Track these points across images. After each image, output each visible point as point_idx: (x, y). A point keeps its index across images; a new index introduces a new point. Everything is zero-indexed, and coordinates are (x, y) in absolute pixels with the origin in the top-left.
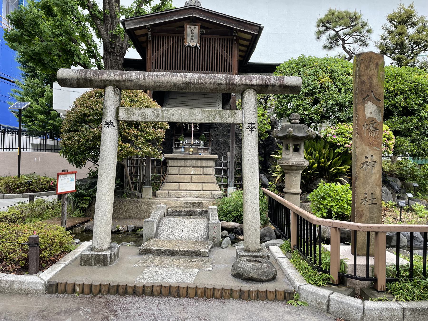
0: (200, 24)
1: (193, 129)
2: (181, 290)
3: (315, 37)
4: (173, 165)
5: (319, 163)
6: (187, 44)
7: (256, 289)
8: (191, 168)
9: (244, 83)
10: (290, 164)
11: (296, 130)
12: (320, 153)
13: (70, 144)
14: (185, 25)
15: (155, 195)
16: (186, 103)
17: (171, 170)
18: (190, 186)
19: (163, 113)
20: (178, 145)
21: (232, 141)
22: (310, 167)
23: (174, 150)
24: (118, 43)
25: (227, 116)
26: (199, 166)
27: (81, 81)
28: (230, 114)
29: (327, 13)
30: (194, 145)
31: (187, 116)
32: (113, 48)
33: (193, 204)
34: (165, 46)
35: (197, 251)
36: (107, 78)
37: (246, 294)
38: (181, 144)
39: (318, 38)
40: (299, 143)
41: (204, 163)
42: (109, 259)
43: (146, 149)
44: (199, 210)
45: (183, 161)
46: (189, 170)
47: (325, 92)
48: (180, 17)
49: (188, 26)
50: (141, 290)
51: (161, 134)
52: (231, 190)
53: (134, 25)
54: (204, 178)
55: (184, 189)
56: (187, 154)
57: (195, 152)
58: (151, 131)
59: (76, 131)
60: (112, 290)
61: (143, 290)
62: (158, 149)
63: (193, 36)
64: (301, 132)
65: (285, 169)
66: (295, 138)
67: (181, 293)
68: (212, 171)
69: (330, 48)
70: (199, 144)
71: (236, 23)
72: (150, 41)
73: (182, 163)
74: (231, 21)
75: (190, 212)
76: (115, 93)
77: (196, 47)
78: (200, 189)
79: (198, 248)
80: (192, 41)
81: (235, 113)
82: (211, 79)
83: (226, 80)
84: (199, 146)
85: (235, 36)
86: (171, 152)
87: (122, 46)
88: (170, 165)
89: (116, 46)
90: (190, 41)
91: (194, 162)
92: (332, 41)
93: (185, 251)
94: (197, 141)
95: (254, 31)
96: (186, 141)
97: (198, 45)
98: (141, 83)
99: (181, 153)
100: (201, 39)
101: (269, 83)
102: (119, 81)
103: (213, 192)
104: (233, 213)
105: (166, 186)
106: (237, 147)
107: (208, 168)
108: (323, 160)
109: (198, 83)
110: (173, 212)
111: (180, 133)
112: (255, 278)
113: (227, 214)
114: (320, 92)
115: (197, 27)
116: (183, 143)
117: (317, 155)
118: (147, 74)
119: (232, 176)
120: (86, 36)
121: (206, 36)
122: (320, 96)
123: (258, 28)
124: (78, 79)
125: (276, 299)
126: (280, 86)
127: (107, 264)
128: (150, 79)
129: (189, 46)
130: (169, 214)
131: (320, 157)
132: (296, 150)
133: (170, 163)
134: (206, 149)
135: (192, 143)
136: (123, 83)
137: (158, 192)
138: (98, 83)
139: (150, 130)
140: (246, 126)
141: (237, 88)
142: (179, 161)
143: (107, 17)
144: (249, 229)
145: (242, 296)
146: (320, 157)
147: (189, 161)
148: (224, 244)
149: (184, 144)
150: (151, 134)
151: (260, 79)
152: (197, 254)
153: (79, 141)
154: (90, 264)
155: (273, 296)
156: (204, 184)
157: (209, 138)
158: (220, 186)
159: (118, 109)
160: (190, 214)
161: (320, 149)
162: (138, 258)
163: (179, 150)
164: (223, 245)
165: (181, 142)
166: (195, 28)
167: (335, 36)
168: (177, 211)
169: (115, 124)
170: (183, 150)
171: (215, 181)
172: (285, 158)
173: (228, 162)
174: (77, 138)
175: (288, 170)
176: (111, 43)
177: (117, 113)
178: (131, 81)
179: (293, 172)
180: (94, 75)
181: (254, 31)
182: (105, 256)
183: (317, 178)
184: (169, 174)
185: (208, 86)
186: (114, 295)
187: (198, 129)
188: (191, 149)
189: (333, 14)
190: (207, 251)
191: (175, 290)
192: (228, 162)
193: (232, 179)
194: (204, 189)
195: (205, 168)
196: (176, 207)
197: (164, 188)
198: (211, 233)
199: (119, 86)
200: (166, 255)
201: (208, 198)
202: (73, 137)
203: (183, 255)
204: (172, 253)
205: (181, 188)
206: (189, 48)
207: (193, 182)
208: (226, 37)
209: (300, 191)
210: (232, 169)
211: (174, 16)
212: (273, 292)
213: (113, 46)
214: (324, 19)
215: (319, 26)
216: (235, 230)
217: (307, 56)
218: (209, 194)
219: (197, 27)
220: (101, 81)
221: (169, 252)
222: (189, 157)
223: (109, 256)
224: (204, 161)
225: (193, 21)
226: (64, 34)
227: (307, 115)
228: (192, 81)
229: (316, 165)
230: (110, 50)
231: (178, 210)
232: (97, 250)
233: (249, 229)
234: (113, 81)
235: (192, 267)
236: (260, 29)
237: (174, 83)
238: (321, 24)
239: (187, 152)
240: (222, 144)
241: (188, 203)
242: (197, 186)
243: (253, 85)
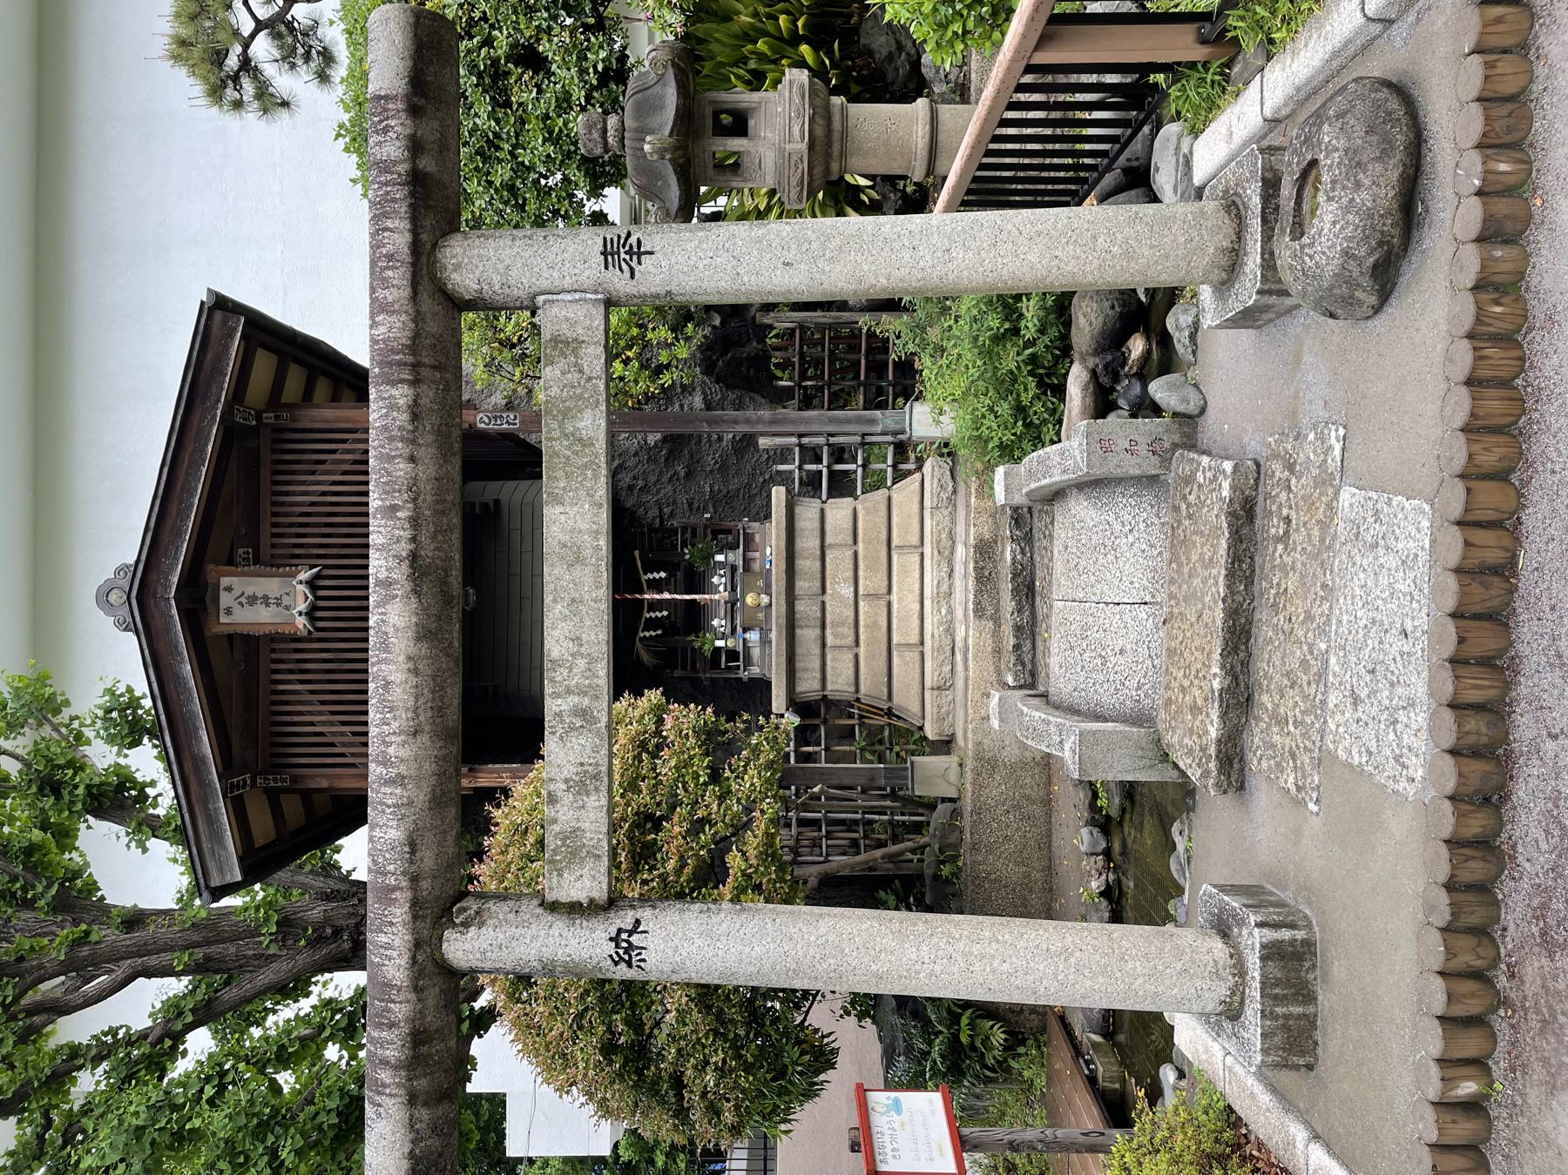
0: (211, 566)
1: (666, 596)
2: (1478, 557)
3: (284, 114)
4: (818, 675)
5: (795, 40)
6: (301, 622)
7: (1474, 160)
8: (827, 598)
9: (406, 292)
10: (804, 146)
11: (653, 122)
12: (749, 36)
13: (737, 1107)
14: (217, 630)
15: (945, 746)
17: (839, 683)
18: (904, 599)
19: (569, 692)
20: (733, 655)
21: (709, 423)
22: (818, 73)
23: (755, 671)
24: (317, 913)
25: (573, 377)
26: (818, 564)
27: (422, 1084)
28: (562, 364)
29: (184, 70)
30: (733, 589)
31: (578, 571)
32: (337, 932)
33: (984, 579)
34: (311, 713)
35: (1232, 515)
36: (404, 961)
37: (1502, 206)
38: (731, 643)
39: (285, 104)
40: (709, 111)
41: (807, 543)
42: (1285, 934)
43: (749, 779)
44: (1008, 552)
45: (798, 632)
46: (839, 609)
47: (484, 18)
49: (223, 619)
50: (1477, 767)
51: (685, 719)
52: (922, 421)
53: (225, 848)
54: (868, 542)
55: (916, 623)
57: (761, 583)
59: (678, 1083)
60: (1475, 918)
61: (1475, 753)
62: (748, 732)
63: (266, 598)
64: (661, 98)
65: (827, 171)
66: (687, 121)
67: (1494, 556)
68: (839, 511)
69: (327, 57)
71: (197, 415)
72: (295, 779)
73: (807, 635)
74: (191, 434)
75: (1018, 589)
76: (478, 919)
77: (311, 584)
78: (917, 558)
79: (1214, 516)
80: (286, 601)
81: (555, 340)
82: (390, 459)
83: (393, 383)
84: (734, 569)
85: (258, 416)
86: (763, 685)
87: (327, 897)
88: (816, 685)
89: (327, 920)
90: (287, 608)
91: (802, 585)
92: (301, 50)
93: (1230, 575)
94: (715, 580)
95: (235, 330)
96: (715, 622)
97: (305, 575)
98: (422, 797)
99: (765, 641)
100: (276, 561)
101: (403, 168)
102: (415, 904)
103: (927, 503)
104: (1025, 399)
105: (906, 699)
107: (828, 527)
108: (783, 20)
109: (415, 522)
110: (1020, 661)
111: (685, 650)
112: (1403, 178)
113: (1027, 425)
114: (488, 42)
115: (225, 581)
116: (723, 637)
117: (761, 45)
118: (381, 770)
119: (859, 420)
120: (282, 1047)
121: (265, 540)
122: (502, 41)
123: (218, 315)
124: (412, 1100)
125: (1522, 49)
126: (414, 111)
127: (1308, 944)
128: (404, 753)
129: (310, 614)
130: (1031, 680)
131: (765, 34)
132: (739, 124)
133: (808, 685)
134: (749, 539)
135: (722, 595)
136: (425, 884)
137: (931, 732)
138: (431, 1002)
139: (667, 766)
140: (619, 282)
141: (432, 327)
142: (799, 651)
143: (207, 958)
144: (1129, 255)
145: (1509, 227)
146: (765, 34)
147: (800, 607)
148: (1185, 400)
149: (728, 631)
151: (386, 215)
152: (1244, 513)
153: (722, 1071)
154: (1311, 1022)
155: (1506, 65)
156: (895, 541)
157: (700, 531)
158: (900, 476)
159: (553, 907)
160: (1027, 589)
161: (735, 36)
162: (1262, 796)
163: (756, 652)
164: (1192, 408)
165: (720, 643)
166: (229, 589)
167: (276, 36)
168: (1017, 647)
169: (626, 919)
170: (753, 636)
171: (881, 494)
172: (779, 171)
173: (800, 445)
174: (710, 1078)
175: (828, 156)
176: (317, 941)
177: (574, 910)
178: (413, 845)
179: (836, 135)
180: (392, 1025)
181: (231, 336)
182: (1271, 952)
183: (860, 54)
184: (857, 691)
185: (427, 471)
186: (1496, 904)
187: (663, 575)
188: (750, 599)
189: (183, 43)
190: (1228, 466)
191: (1476, 588)
192: (800, 445)
193: (873, 421)
194: (915, 540)
195: (829, 540)
196: (997, 652)
197: (915, 707)
198: (1132, 466)
199: (443, 901)
200: (1245, 664)
201: (953, 522)
202: (704, 1095)
203: (1249, 581)
204: (1239, 636)
205: (915, 639)
206: (319, 614)
209: (922, 103)
210: (831, 421)
211: (178, 678)
212: (1489, 65)
213: (329, 931)
214: (206, 79)
215: (238, 105)
216: (1105, 380)
217: (345, 117)
218: (938, 516)
219: (225, 581)
220: (417, 989)
221: (1235, 650)
222: (783, 609)
223: (1270, 935)
225: (197, 599)
226: (271, 1139)
227: (588, 97)
228: (404, 548)
229: (805, 49)
230: (347, 946)
231: (1012, 641)
232: (1238, 991)
233: (1129, 255)
234: (415, 931)
235: (1324, 525)
236: (219, 308)
237: (419, 638)
238: (230, 93)
240: (726, 482)
241: (977, 604)
242: (905, 572)
243: (416, 248)
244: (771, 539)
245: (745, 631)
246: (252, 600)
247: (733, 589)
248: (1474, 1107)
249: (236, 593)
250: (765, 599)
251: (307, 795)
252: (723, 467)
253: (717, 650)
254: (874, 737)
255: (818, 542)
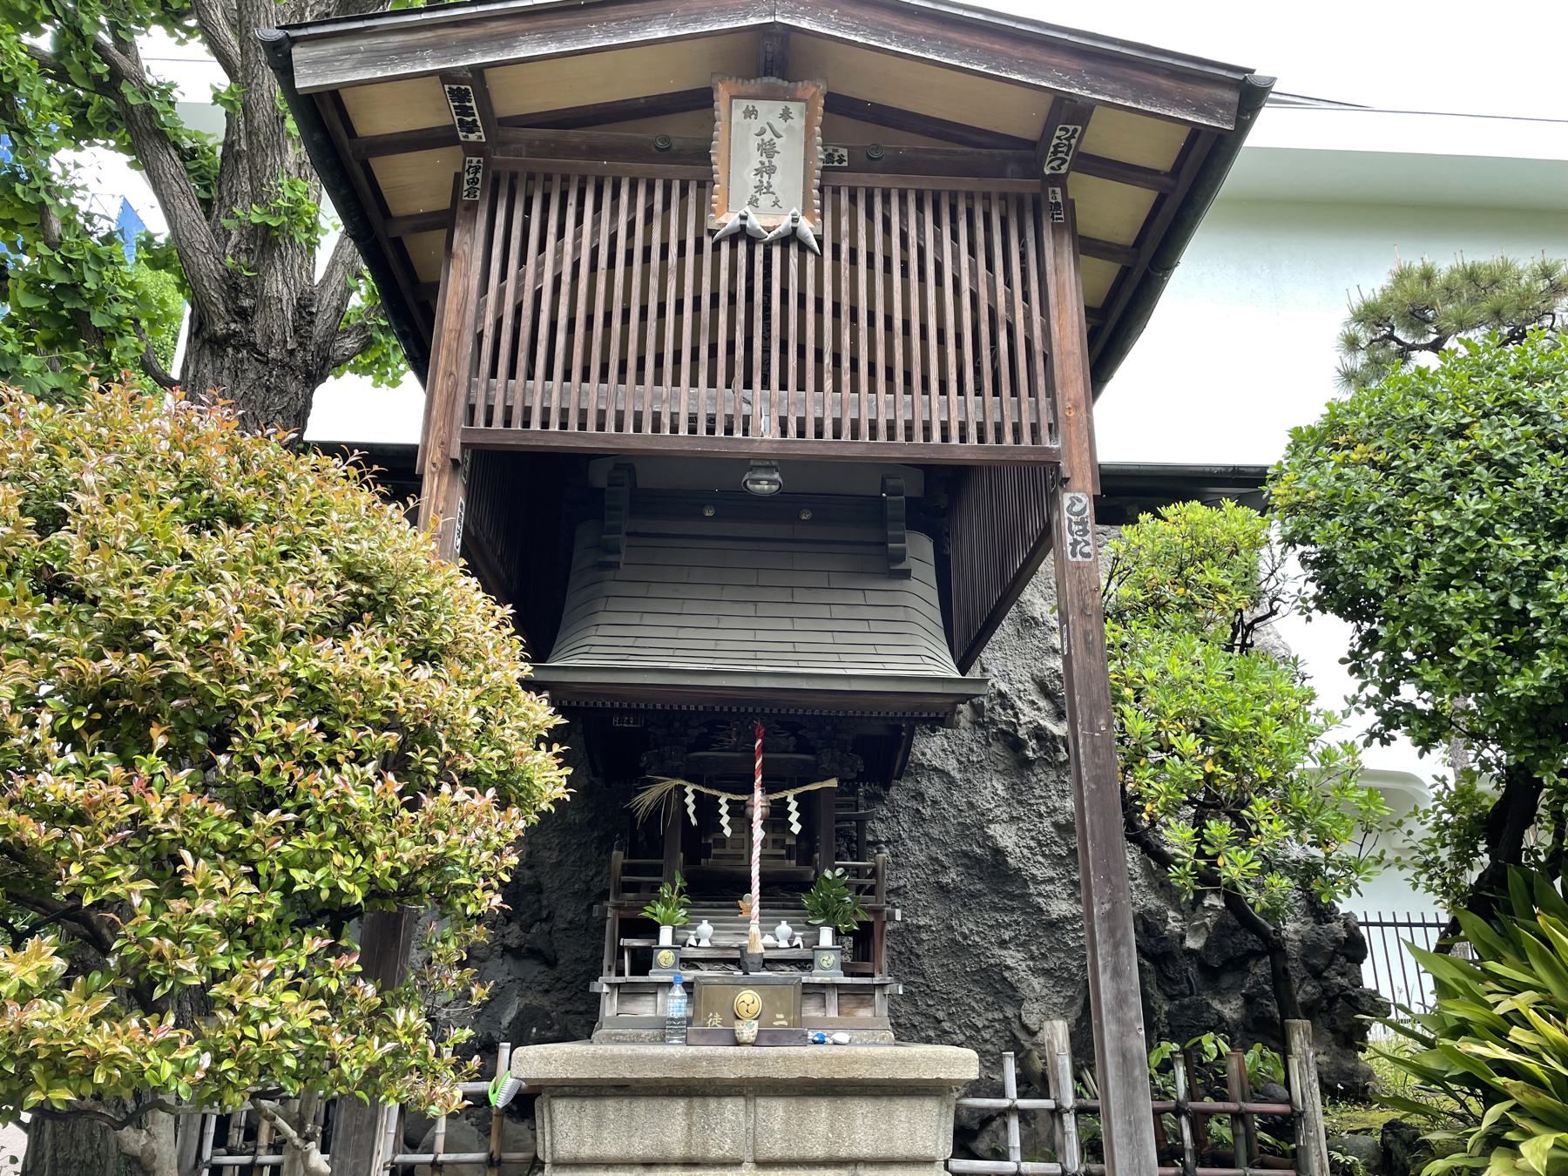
1: (758, 834)
4: (586, 1152)
6: (729, 220)
16: (711, 645)
20: (643, 962)
21: (1109, 916)
23: (610, 1007)
24: (276, 285)
26: (820, 1152)
30: (768, 963)
32: (243, 315)
34: (578, 236)
38: (665, 957)
43: (276, 1005)
45: (680, 1105)
48: (684, 25)
49: (740, 106)
51: (480, 840)
53: (354, 68)
56: (711, 1037)
57: (781, 1021)
58: (358, 801)
63: (771, 170)
70: (802, 953)
72: (472, 207)
74: (1036, 53)
80: (765, 201)
84: (805, 964)
86: (578, 1022)
88: (566, 1149)
89: (264, 302)
90: (753, 202)
94: (784, 928)
95: (1211, 116)
96: (705, 928)
97: (807, 228)
99: (664, 1029)
106: (1034, 971)
111: (657, 870)
116: (679, 944)
121: (863, 180)
123: (1231, 96)
129: (742, 235)
134: (861, 995)
139: (361, 791)
142: (641, 1107)
147: (732, 1109)
149: (689, 953)
150: (353, 837)
157: (871, 901)
163: (644, 1008)
166: (786, 115)
170: (675, 1004)
173: (1057, 1112)
181: (1200, 110)
187: (796, 828)
188: (749, 999)
192: (1057, 1112)
206: (742, 248)
208: (994, 185)
213: (246, 303)
215: (1352, 344)
219: (795, 108)
222: (728, 1073)
224: (862, 1109)
239: (715, 1021)
240: (934, 952)
244: (860, 1044)
245: (688, 986)
246: (768, 150)
247: (768, 963)
249: (780, 125)
250: (748, 1030)
252: (958, 948)
253: (652, 930)
255: (865, 1151)
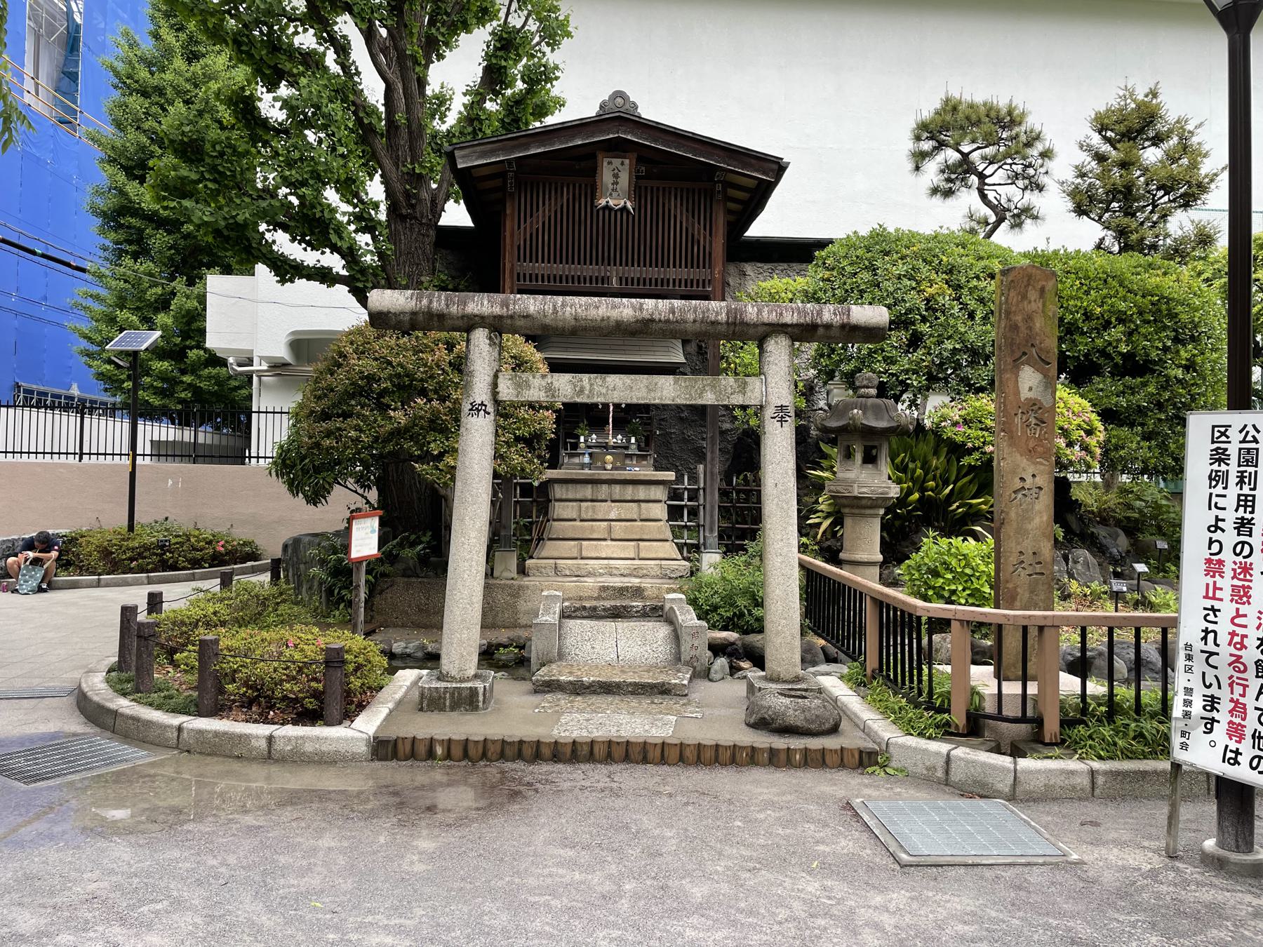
0: (635, 155)
2: (650, 750)
3: (911, 166)
5: (923, 490)
6: (603, 202)
7: (802, 746)
8: (609, 503)
9: (766, 321)
10: (856, 494)
11: (869, 413)
12: (925, 466)
13: (333, 448)
14: (600, 157)
15: (522, 571)
17: (559, 510)
18: (608, 548)
19: (591, 385)
20: (575, 446)
22: (902, 501)
23: (566, 460)
24: (425, 195)
25: (729, 390)
27: (421, 318)
28: (735, 386)
29: (939, 106)
30: (614, 448)
31: (644, 390)
33: (622, 591)
35: (663, 684)
36: (476, 311)
37: (783, 757)
38: (582, 445)
39: (917, 168)
40: (876, 443)
41: (642, 492)
42: (481, 698)
44: (638, 604)
46: (603, 510)
47: (937, 318)
50: (568, 750)
52: (711, 560)
53: (477, 159)
54: (642, 528)
55: (594, 555)
56: (598, 468)
57: (618, 464)
59: (346, 415)
60: (508, 752)
61: (574, 751)
62: (539, 457)
64: (882, 419)
65: (845, 506)
66: (868, 433)
67: (650, 756)
68: (660, 511)
69: (948, 193)
71: (721, 153)
72: (512, 195)
73: (588, 491)
75: (617, 608)
76: (492, 344)
77: (625, 208)
78: (632, 556)
79: (661, 678)
81: (746, 383)
82: (695, 311)
83: (727, 314)
84: (626, 448)
85: (719, 182)
87: (433, 201)
88: (558, 496)
89: (419, 200)
91: (617, 489)
92: (953, 176)
93: (635, 684)
94: (620, 437)
97: (629, 205)
98: (547, 321)
99: (583, 466)
100: (637, 191)
101: (819, 321)
102: (501, 317)
103: (664, 562)
104: (721, 611)
105: (550, 548)
107: (651, 505)
108: (932, 484)
109: (668, 321)
110: (577, 609)
112: (797, 727)
113: (707, 613)
114: (924, 320)
115: (627, 161)
116: (586, 441)
117: (919, 471)
118: (560, 303)
119: (712, 523)
120: (354, 181)
122: (924, 328)
123: (775, 167)
124: (414, 313)
125: (842, 765)
126: (843, 326)
127: (476, 708)
128: (567, 314)
130: (565, 615)
131: (926, 475)
132: (870, 459)
133: (559, 491)
134: (644, 457)
135: (611, 441)
136: (509, 321)
137: (529, 563)
138: (456, 322)
140: (769, 412)
141: (751, 331)
143: (397, 128)
144: (778, 633)
145: (775, 760)
146: (926, 475)
147: (605, 487)
148: (716, 672)
151: (799, 313)
152: (663, 690)
153: (356, 440)
154: (442, 709)
155: (836, 758)
156: (641, 543)
158: (680, 547)
159: (496, 376)
160: (616, 614)
161: (925, 457)
162: (536, 699)
163: (576, 460)
164: (712, 675)
165: (582, 439)
166: (622, 164)
167: (960, 164)
168: (584, 608)
169: (490, 409)
170: (587, 459)
171: (669, 535)
172: (845, 480)
174: (353, 434)
175: (852, 507)
176: (408, 195)
177: (495, 385)
178: (527, 316)
179: (863, 511)
180: (447, 306)
182: (474, 691)
183: (917, 526)
185: (689, 327)
186: (513, 760)
188: (609, 458)
189: (955, 109)
190: (685, 682)
191: (638, 749)
193: (711, 531)
194: (642, 555)
195: (643, 505)
196: (581, 599)
197: (544, 554)
198: (685, 647)
199: (497, 326)
200: (594, 692)
201: (653, 577)
202: (339, 429)
203: (632, 693)
204: (607, 689)
205: (585, 554)
207: (620, 538)
209: (880, 558)
210: (712, 507)
211: (573, 137)
212: (836, 751)
214: (933, 120)
215: (918, 138)
216: (729, 649)
217: (891, 230)
218: (656, 569)
219: (627, 161)
220: (463, 317)
221: (601, 687)
223: (481, 691)
224: (641, 488)
225: (617, 148)
226: (311, 182)
227: (892, 374)
228: (656, 317)
229: (916, 496)
230: (404, 211)
231: (588, 605)
232: (453, 679)
233: (778, 633)
234: (489, 317)
235: (660, 713)
236: (777, 168)
237: (617, 322)
238: (926, 135)
239: (599, 464)
241: (608, 588)
242: (624, 548)
243: (785, 325)
244: (644, 471)
245: (590, 454)
246: (616, 176)
247: (614, 448)
248: (431, 755)
249: (620, 167)
250: (609, 467)
251: (502, 203)
252: (686, 441)
253: (578, 438)
254: (528, 528)
255: (642, 498)
